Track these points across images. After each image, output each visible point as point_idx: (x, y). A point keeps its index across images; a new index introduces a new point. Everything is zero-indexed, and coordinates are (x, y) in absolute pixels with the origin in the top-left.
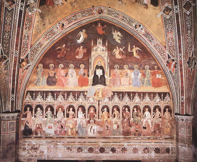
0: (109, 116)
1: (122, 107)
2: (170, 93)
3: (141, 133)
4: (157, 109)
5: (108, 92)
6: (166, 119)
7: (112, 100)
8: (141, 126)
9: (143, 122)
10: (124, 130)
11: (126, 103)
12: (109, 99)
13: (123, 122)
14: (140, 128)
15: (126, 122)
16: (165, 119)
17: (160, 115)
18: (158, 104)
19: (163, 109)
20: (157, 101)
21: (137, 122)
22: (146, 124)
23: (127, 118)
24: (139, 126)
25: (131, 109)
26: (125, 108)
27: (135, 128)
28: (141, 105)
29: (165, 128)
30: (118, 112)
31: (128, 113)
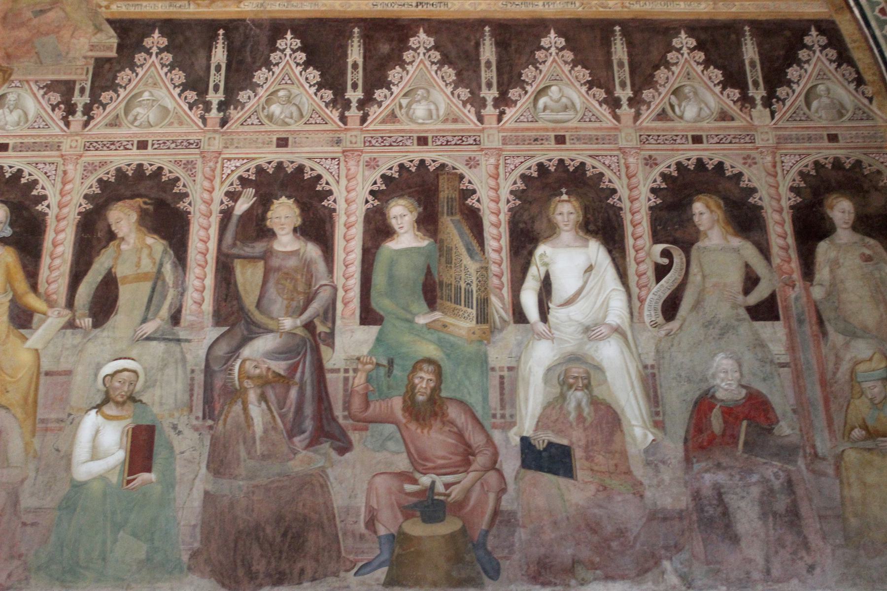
0: (32, 301)
1: (219, 194)
2: (846, 28)
3: (491, 543)
4: (698, 207)
5: (59, 28)
6: (852, 333)
7: (96, 111)
8: (497, 436)
9: (523, 370)
10: (225, 486)
11: (283, 143)
12: (56, 98)
13: (218, 382)
14: (480, 461)
15: (265, 382)
16: (836, 338)
17: (751, 281)
18: (710, 153)
19: (788, 200)
20: (690, 111)
21: (424, 381)
22: (572, 406)
23: (288, 323)
24: (460, 435)
25: (341, 206)
26: (264, 201)
27: (402, 463)
28: (487, 163)
29: (852, 456)
30: (156, 244)
31: (307, 266)
